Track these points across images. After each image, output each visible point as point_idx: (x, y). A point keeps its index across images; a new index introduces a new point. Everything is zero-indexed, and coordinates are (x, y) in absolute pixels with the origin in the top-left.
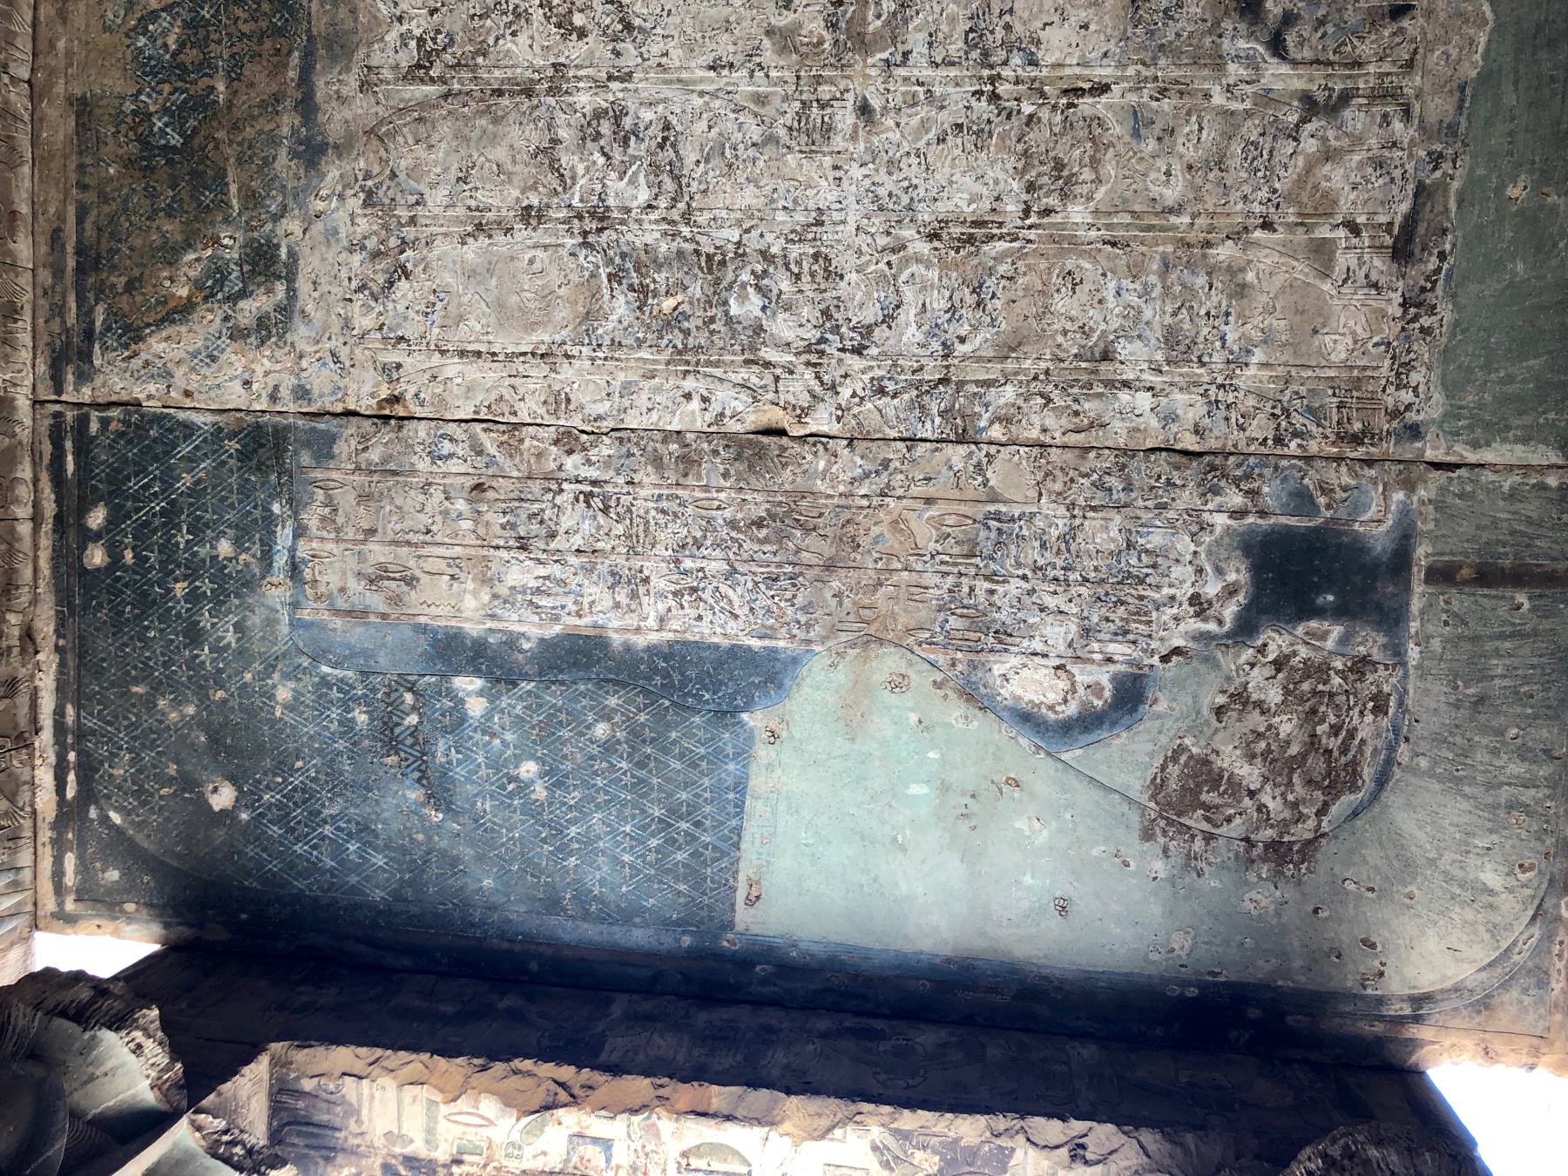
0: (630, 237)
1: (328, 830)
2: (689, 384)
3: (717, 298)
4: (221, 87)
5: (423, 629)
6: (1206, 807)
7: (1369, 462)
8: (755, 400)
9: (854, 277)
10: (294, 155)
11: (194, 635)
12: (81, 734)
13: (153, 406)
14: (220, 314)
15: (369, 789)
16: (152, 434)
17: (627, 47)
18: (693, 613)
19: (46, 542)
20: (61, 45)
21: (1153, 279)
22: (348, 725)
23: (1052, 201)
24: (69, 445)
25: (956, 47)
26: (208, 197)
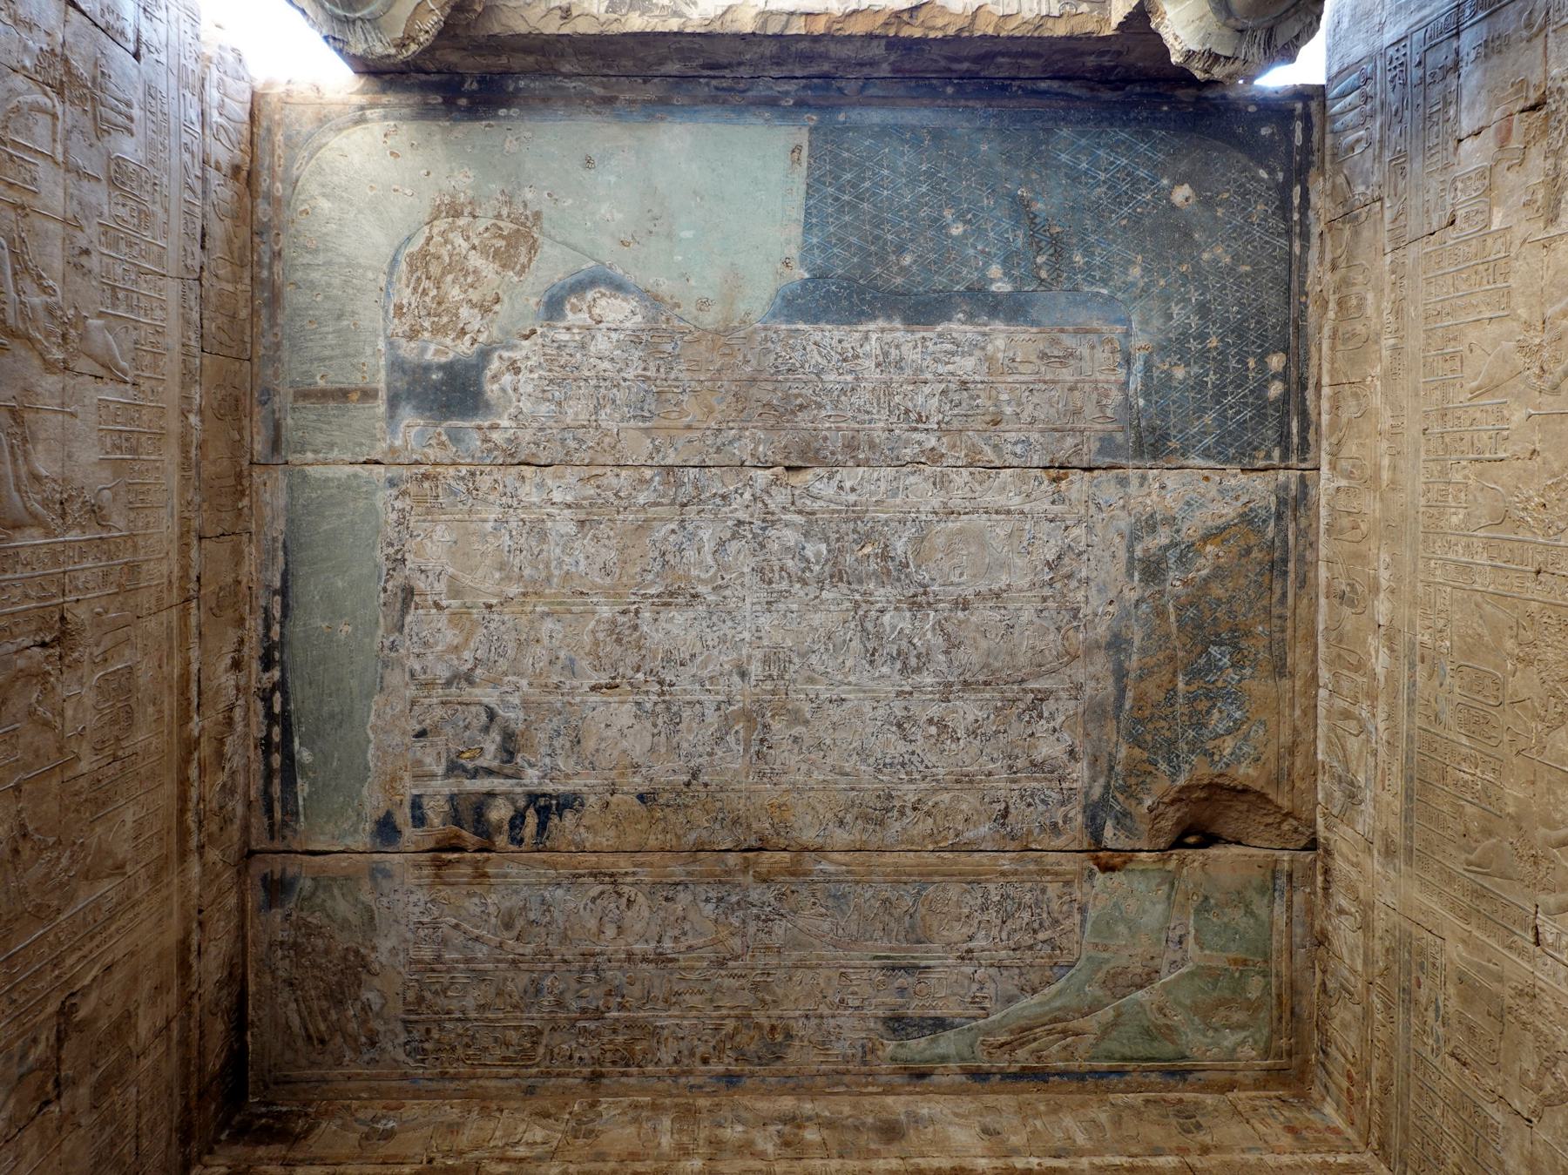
0: (894, 592)
1: (1102, 176)
2: (852, 498)
3: (835, 555)
4: (1181, 685)
5: (1034, 323)
6: (501, 236)
7: (417, 463)
8: (807, 489)
9: (746, 570)
10: (1130, 642)
11: (1203, 310)
12: (1288, 233)
13: (1233, 469)
14: (1182, 534)
15: (1072, 208)
16: (1235, 448)
17: (900, 713)
18: (845, 344)
19: (1313, 370)
20: (1298, 712)
21: (556, 572)
22: (1088, 252)
23: (621, 619)
24: (1295, 440)
25: (687, 713)
26: (1191, 612)
